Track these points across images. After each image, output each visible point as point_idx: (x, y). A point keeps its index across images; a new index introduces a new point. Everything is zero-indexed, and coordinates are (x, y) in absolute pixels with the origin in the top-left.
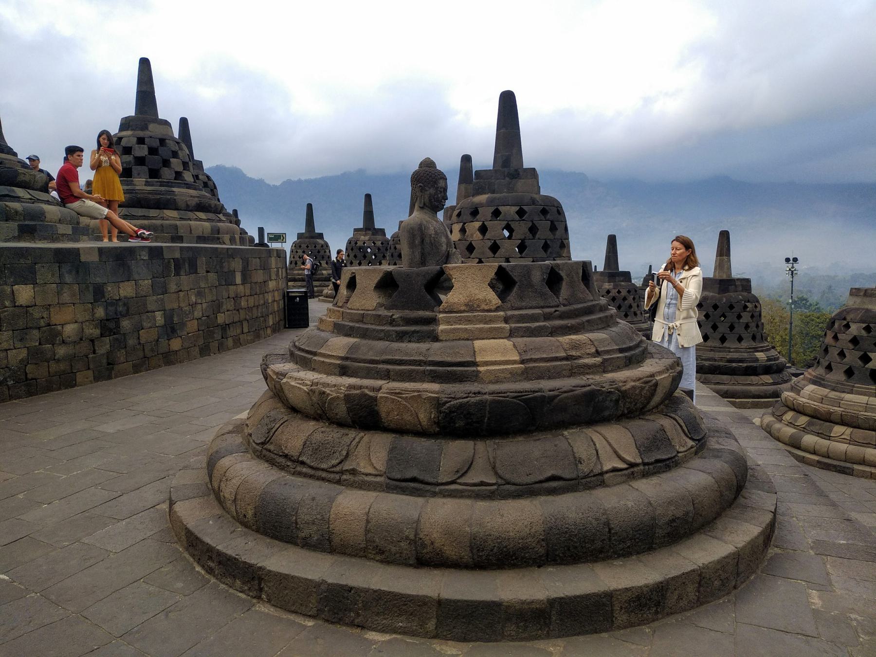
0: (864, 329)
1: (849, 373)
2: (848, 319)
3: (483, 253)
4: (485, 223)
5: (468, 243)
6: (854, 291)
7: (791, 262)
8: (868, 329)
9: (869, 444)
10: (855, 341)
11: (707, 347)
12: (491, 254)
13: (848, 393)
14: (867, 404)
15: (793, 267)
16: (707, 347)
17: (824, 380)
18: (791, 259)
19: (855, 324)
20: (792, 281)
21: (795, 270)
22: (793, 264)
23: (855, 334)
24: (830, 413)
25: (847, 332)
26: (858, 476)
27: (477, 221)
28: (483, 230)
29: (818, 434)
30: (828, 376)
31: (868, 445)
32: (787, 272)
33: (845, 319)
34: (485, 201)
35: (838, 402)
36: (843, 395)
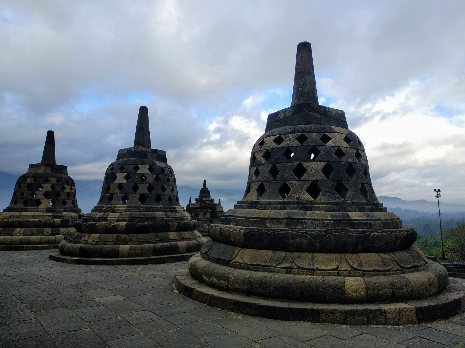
0: (33, 180)
1: (26, 203)
2: (26, 176)
6: (31, 166)
8: (35, 180)
9: (33, 234)
10: (29, 186)
13: (24, 212)
14: (33, 215)
17: (12, 208)
19: (29, 178)
23: (29, 183)
24: (13, 222)
26: (26, 250)
29: (7, 235)
30: (14, 206)
31: (32, 235)
35: (18, 217)
36: (21, 213)
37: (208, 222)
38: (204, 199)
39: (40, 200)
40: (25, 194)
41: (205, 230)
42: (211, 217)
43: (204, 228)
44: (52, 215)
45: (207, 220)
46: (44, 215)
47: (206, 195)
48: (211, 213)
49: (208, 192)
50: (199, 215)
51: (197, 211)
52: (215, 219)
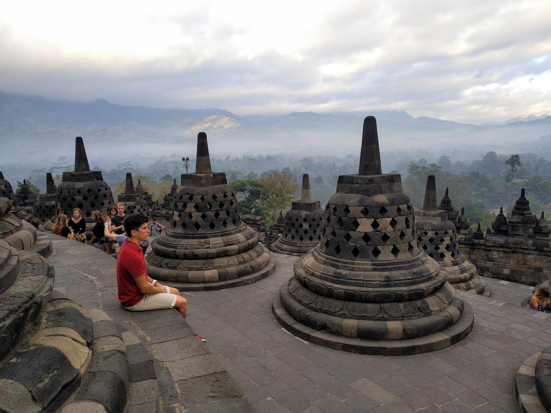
0: (435, 234)
2: (425, 228)
3: (396, 241)
4: (395, 219)
5: (383, 234)
7: (186, 160)
10: (431, 240)
11: (313, 244)
12: (317, 227)
15: (187, 163)
16: (313, 244)
18: (185, 159)
20: (187, 171)
21: (188, 165)
22: (186, 161)
25: (427, 236)
27: (388, 217)
28: (393, 223)
32: (184, 166)
33: (423, 229)
34: (388, 202)
37: (531, 238)
38: (525, 212)
39: (444, 254)
40: (428, 247)
41: (530, 248)
42: (534, 233)
43: (528, 246)
44: (460, 270)
45: (530, 237)
46: (454, 271)
47: (526, 206)
48: (534, 228)
49: (528, 203)
50: (519, 229)
51: (515, 226)
52: (538, 234)
